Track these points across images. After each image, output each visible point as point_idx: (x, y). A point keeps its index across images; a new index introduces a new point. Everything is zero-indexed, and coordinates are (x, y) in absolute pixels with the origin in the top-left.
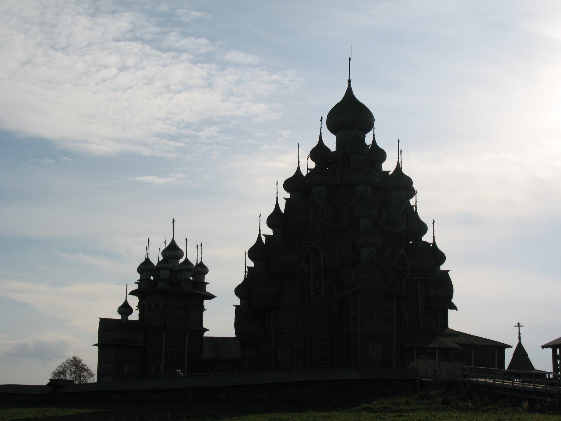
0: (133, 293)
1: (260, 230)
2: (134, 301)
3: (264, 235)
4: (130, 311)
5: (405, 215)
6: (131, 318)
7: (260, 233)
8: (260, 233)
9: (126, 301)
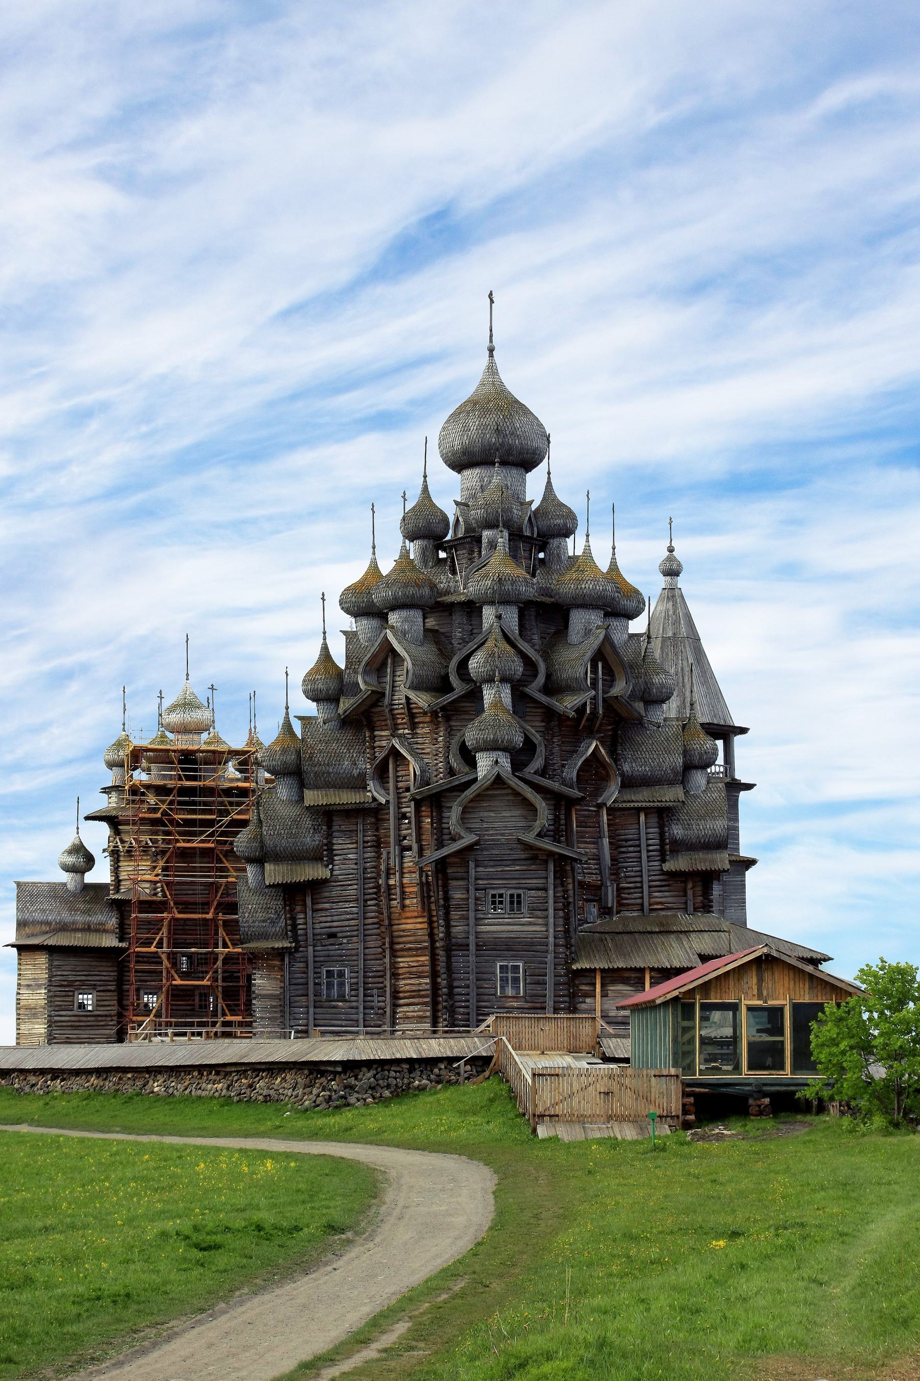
1: (287, 708)
3: (300, 718)
4: (90, 861)
5: (600, 665)
6: (91, 878)
7: (287, 714)
8: (287, 714)
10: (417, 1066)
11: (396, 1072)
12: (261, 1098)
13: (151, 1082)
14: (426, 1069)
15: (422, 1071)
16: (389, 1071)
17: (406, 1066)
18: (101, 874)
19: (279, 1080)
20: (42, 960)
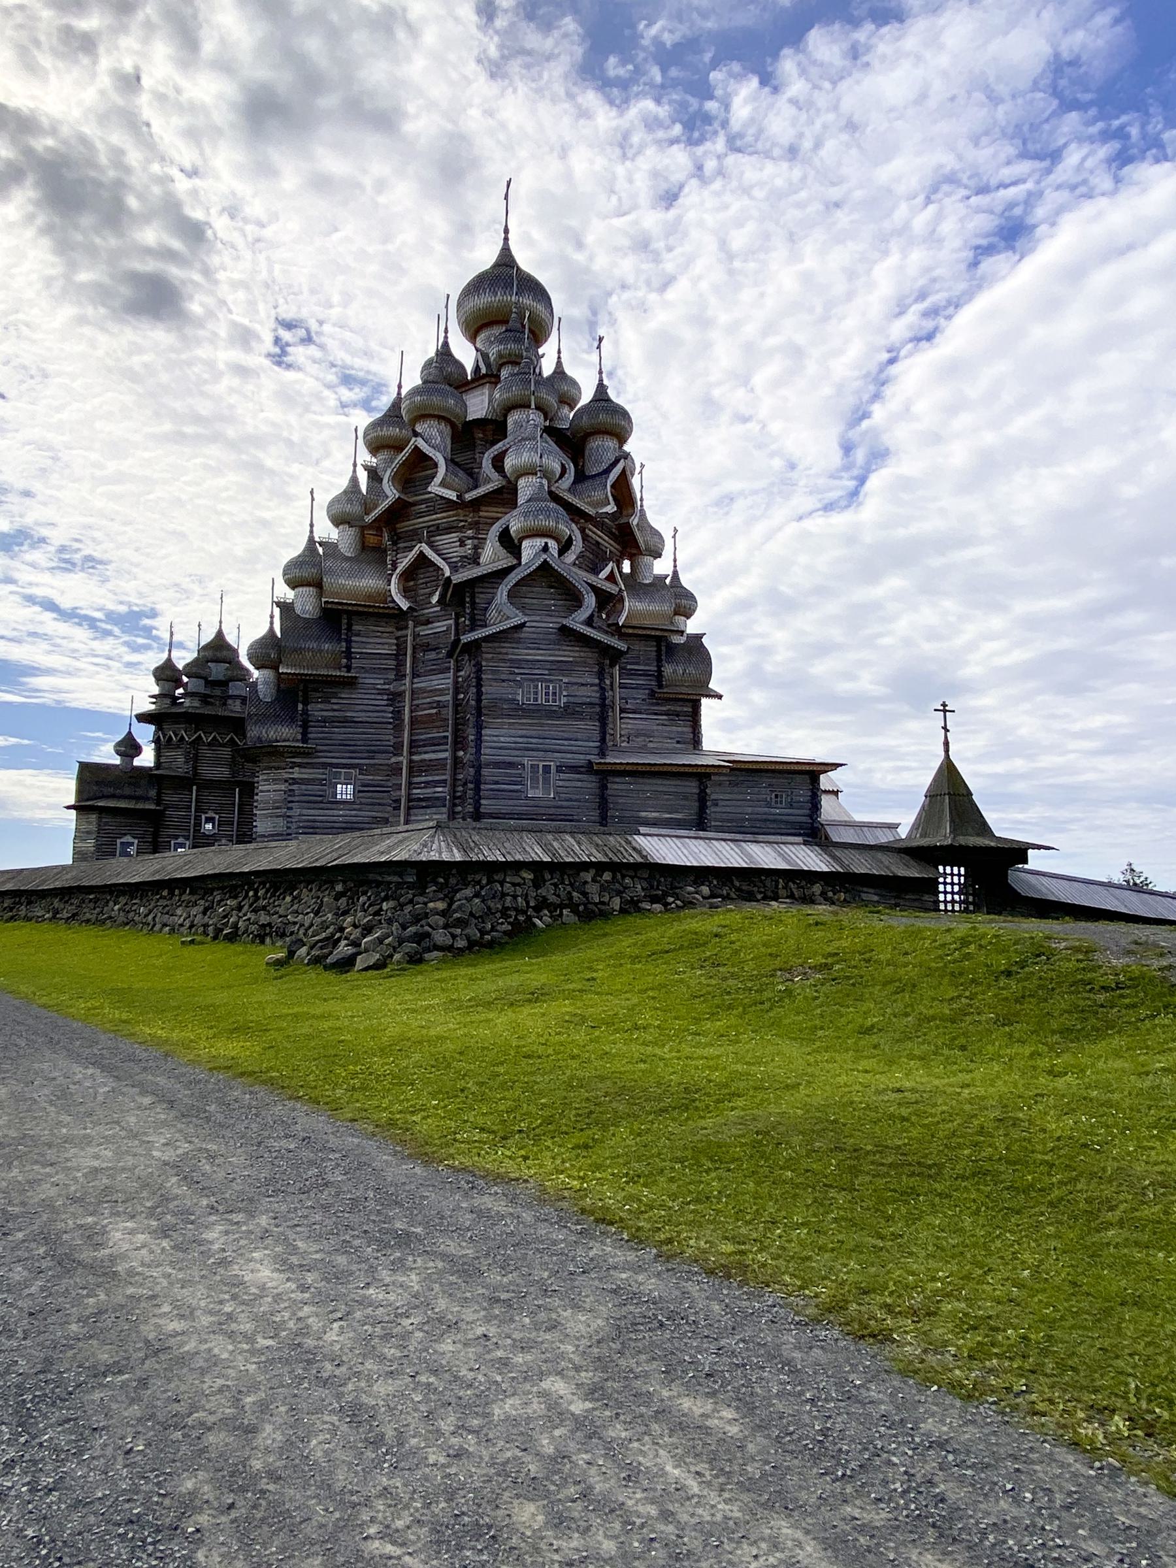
0: (143, 718)
2: (145, 734)
6: (137, 762)
9: (130, 733)
10: (547, 876)
11: (514, 885)
12: (253, 928)
13: (111, 903)
14: (563, 883)
15: (555, 885)
16: (502, 883)
17: (528, 876)
18: (146, 758)
19: (288, 899)
20: (93, 817)
